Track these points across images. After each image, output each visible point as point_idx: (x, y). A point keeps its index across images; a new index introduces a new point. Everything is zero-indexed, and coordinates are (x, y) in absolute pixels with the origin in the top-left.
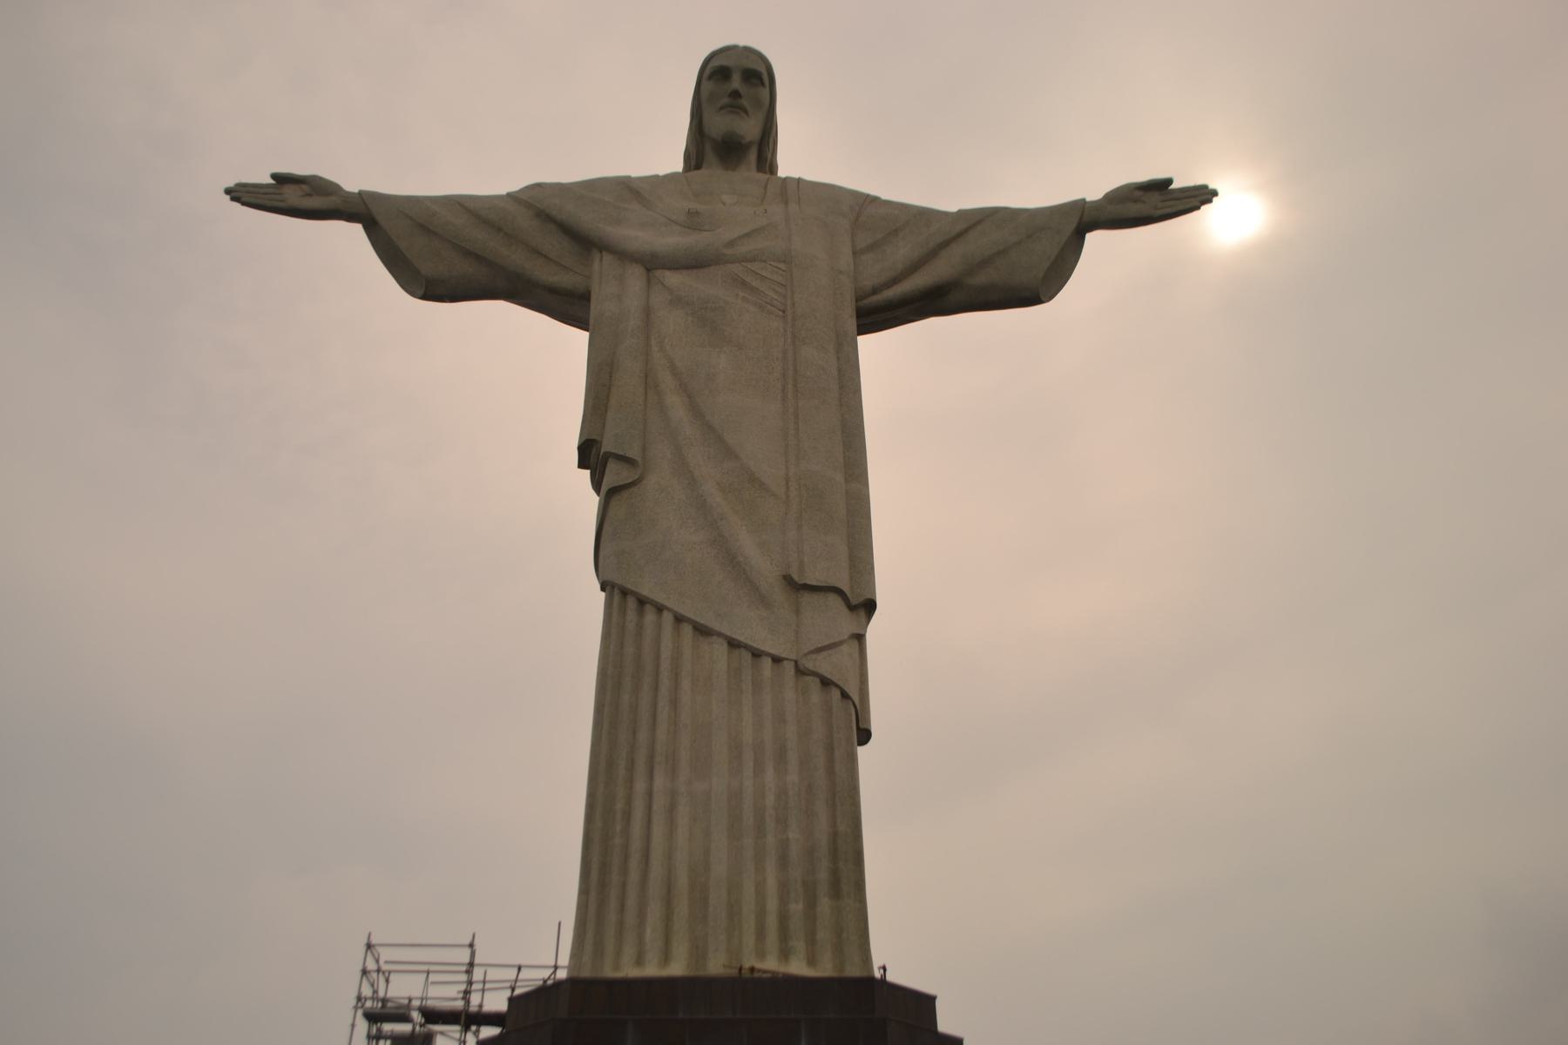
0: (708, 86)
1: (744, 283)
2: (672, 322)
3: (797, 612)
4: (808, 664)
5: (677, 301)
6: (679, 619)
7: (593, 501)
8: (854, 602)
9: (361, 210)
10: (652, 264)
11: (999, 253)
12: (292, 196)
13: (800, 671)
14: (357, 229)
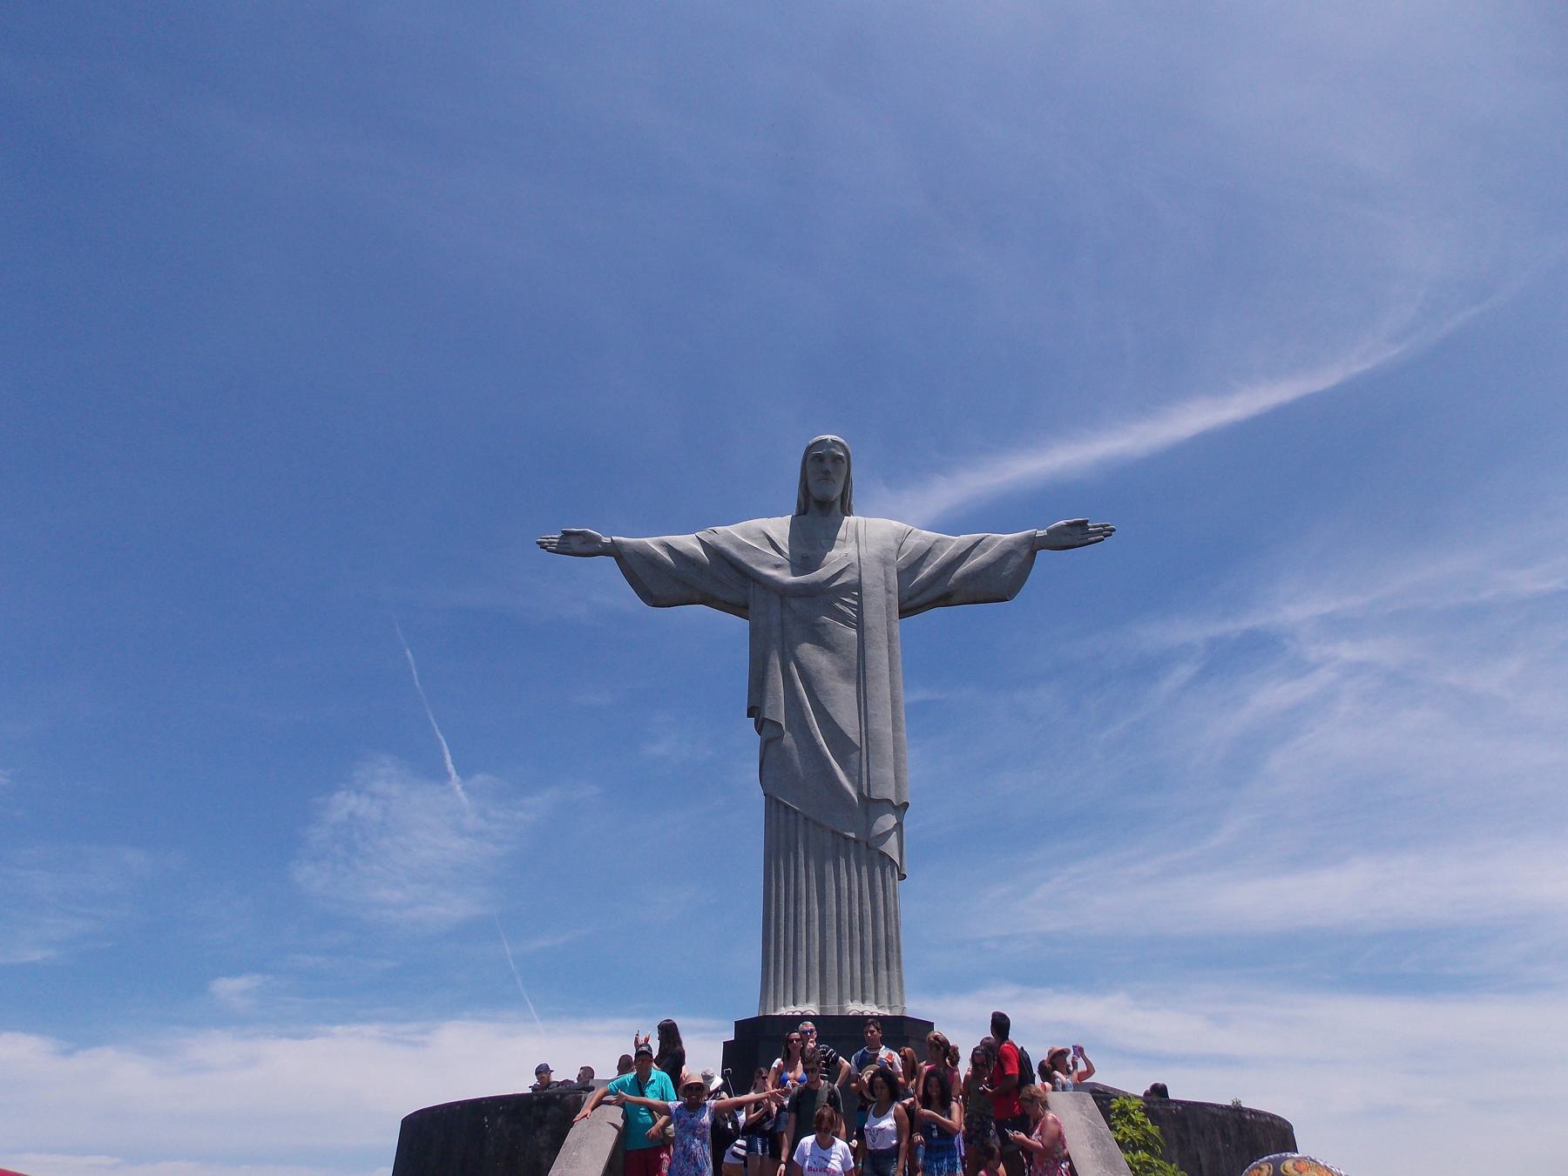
7: (756, 739)
9: (614, 551)
12: (575, 544)
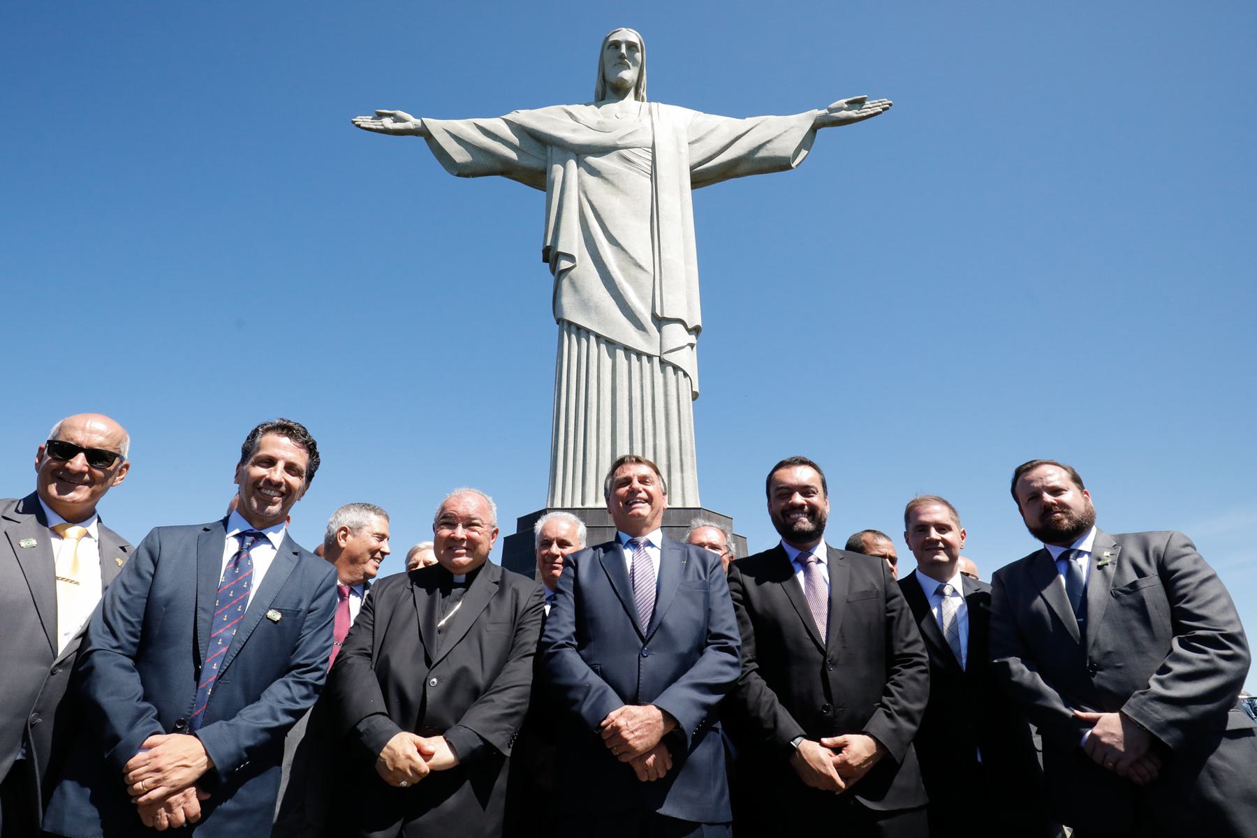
0: (609, 54)
1: (629, 160)
2: (591, 181)
3: (660, 331)
4: (667, 357)
5: (594, 172)
6: (598, 337)
7: (552, 278)
8: (690, 327)
10: (580, 152)
11: (768, 142)
12: (388, 123)
13: (662, 362)
14: (422, 139)
